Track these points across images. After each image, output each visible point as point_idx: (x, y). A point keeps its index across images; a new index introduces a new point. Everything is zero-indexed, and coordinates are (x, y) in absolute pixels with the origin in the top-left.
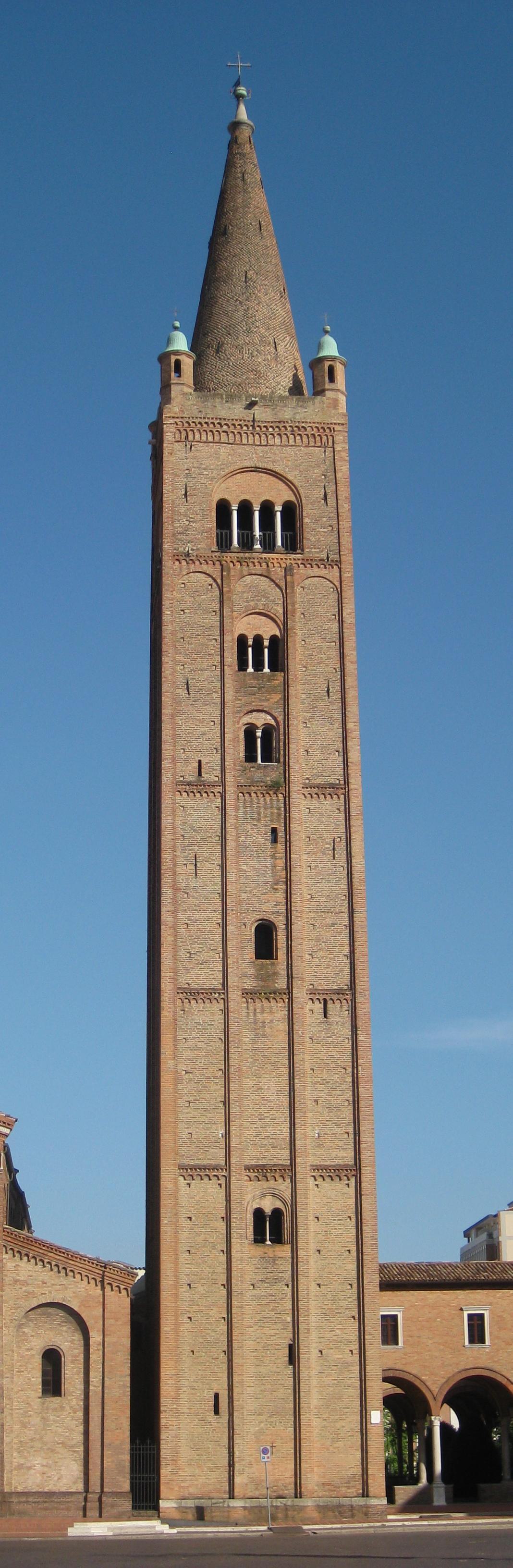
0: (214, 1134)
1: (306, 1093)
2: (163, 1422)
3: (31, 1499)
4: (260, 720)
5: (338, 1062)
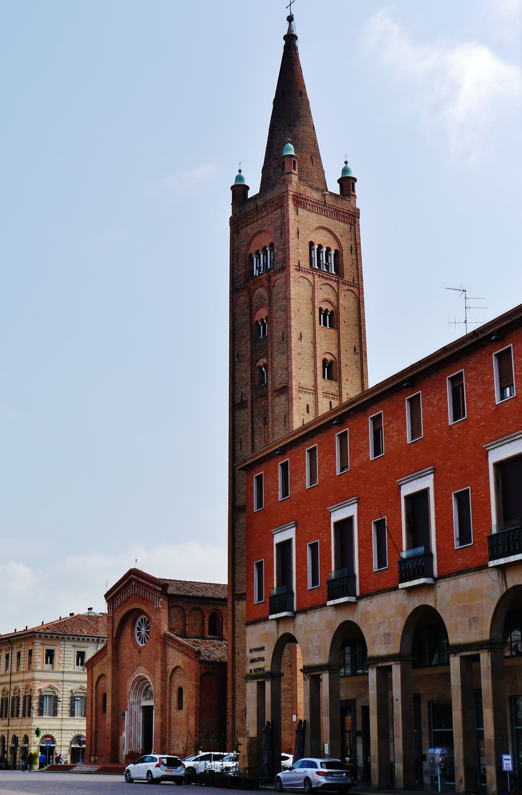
2: (228, 720)
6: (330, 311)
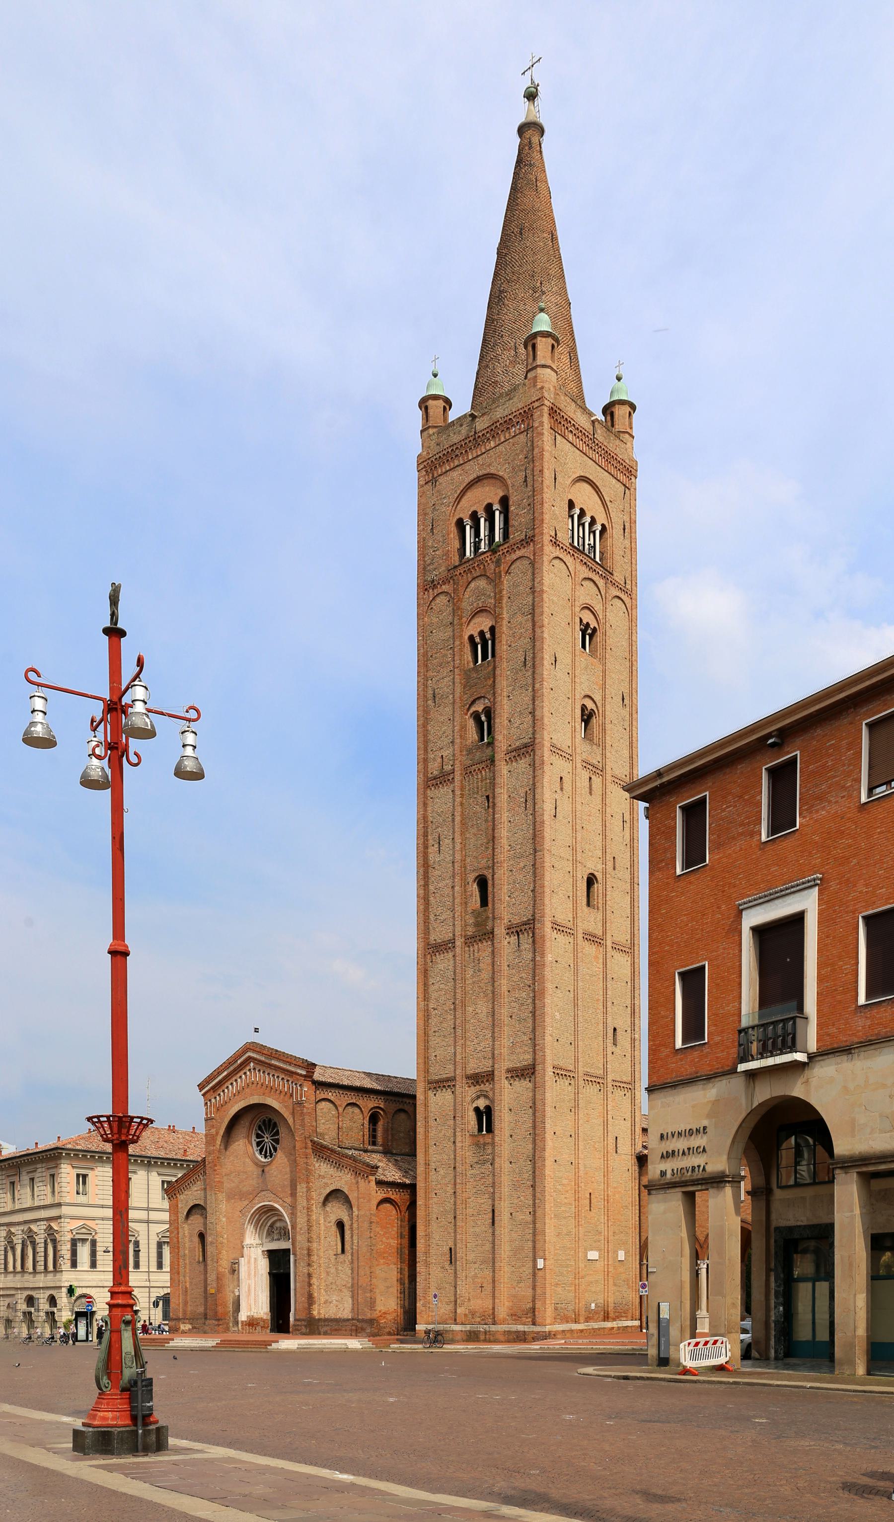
0: (449, 1054)
1: (504, 1012)
2: (418, 1269)
4: (479, 707)
5: (526, 981)
6: (592, 626)
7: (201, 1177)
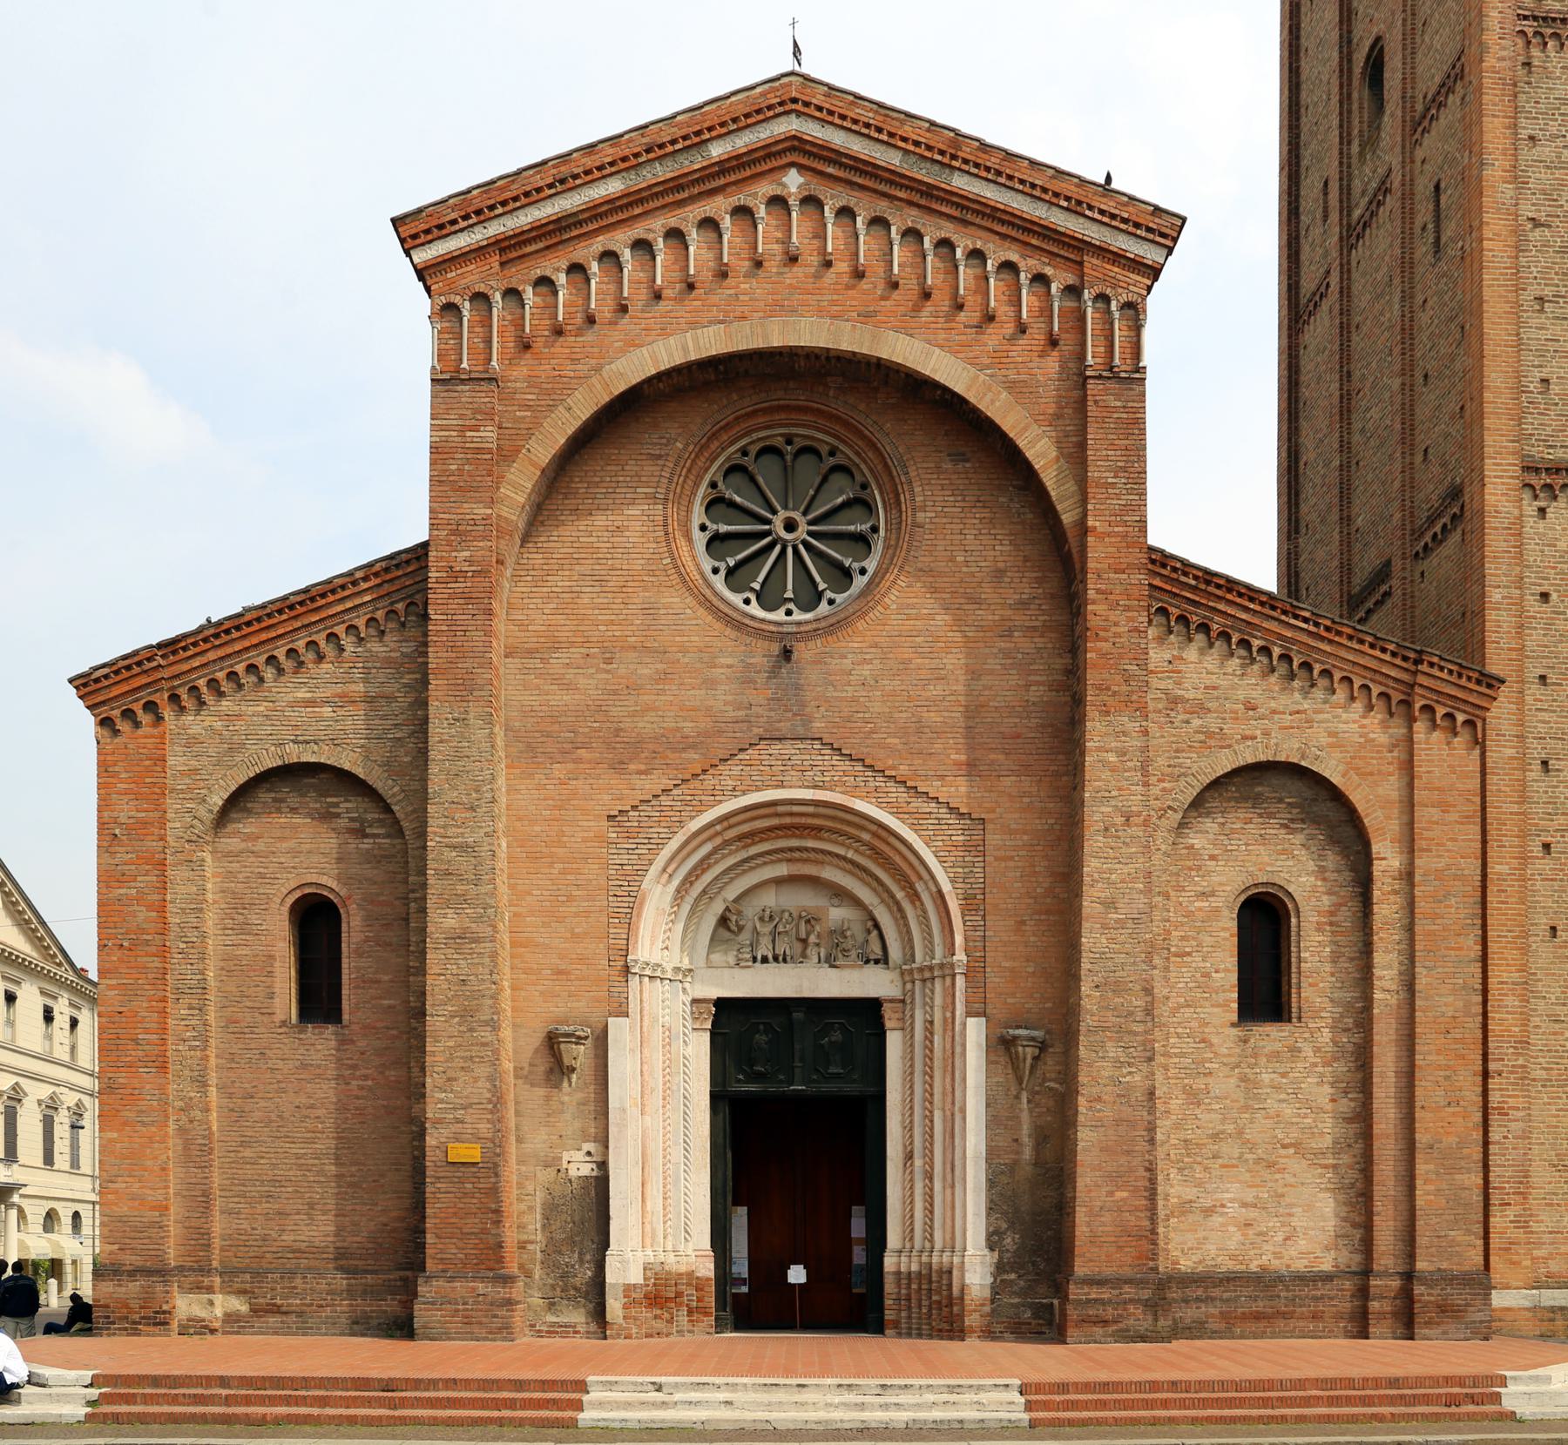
3: (1216, 1292)
7: (348, 642)
